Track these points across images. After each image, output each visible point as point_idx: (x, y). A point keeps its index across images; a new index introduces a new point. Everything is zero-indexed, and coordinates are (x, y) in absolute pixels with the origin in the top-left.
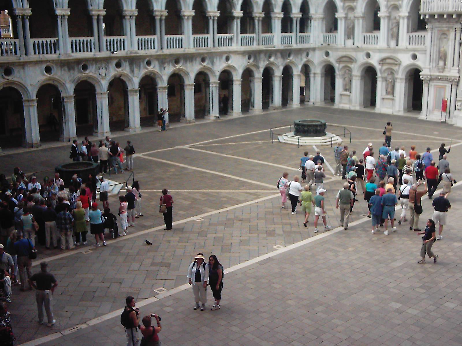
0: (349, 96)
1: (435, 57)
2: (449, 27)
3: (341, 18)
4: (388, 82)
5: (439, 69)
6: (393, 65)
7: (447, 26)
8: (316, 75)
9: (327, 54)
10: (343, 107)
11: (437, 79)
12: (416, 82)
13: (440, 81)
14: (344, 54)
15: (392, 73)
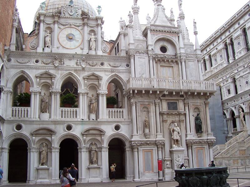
0: (48, 169)
1: (140, 126)
2: (149, 102)
3: (35, 93)
4: (93, 152)
5: (145, 135)
6: (97, 136)
7: (148, 101)
8: (4, 150)
9: (19, 127)
10: (41, 182)
11: (147, 144)
12: (118, 148)
13: (148, 146)
14: (41, 126)
15: (95, 144)
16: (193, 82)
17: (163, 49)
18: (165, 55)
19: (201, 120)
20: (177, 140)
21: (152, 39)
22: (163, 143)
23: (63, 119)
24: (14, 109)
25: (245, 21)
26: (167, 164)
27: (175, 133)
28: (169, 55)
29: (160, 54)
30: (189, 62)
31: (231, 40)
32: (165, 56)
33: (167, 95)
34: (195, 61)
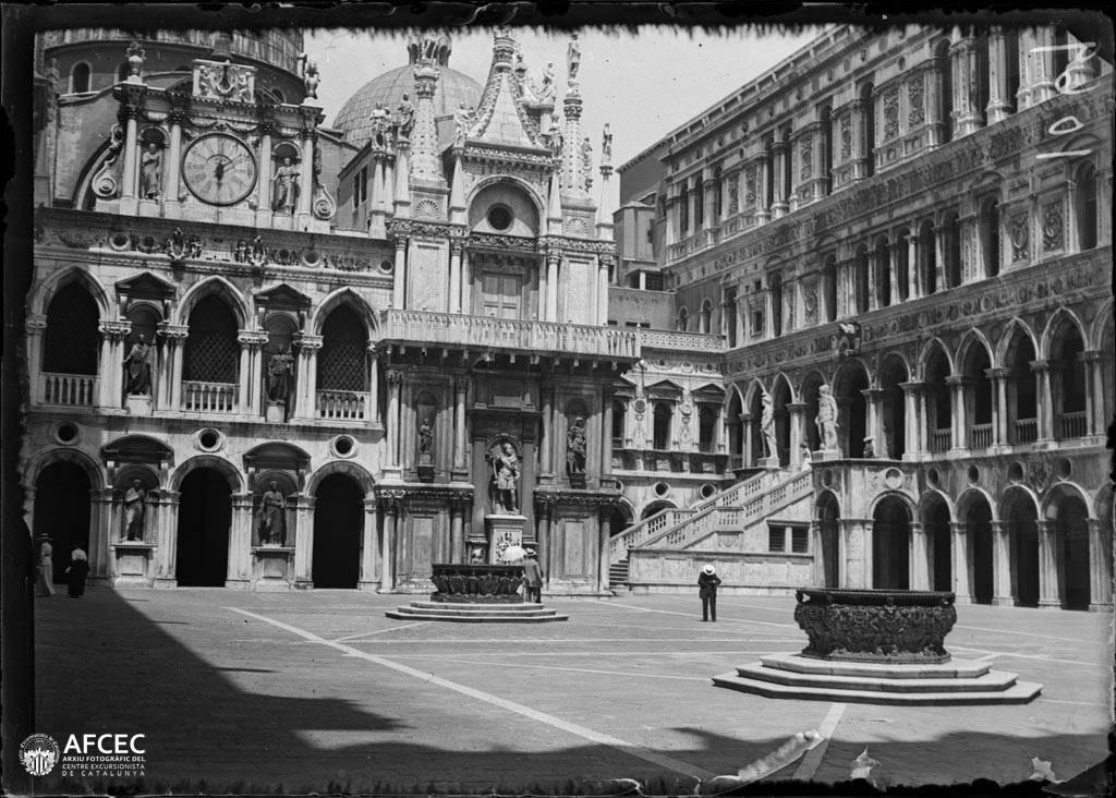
16: (570, 330)
17: (500, 218)
18: (501, 236)
19: (584, 439)
20: (507, 493)
21: (465, 184)
22: (469, 496)
23: (192, 415)
24: (53, 380)
25: (831, 83)
26: (474, 556)
27: (506, 471)
28: (514, 237)
29: (485, 234)
30: (572, 265)
31: (786, 137)
32: (503, 239)
33: (491, 363)
34: (590, 262)
